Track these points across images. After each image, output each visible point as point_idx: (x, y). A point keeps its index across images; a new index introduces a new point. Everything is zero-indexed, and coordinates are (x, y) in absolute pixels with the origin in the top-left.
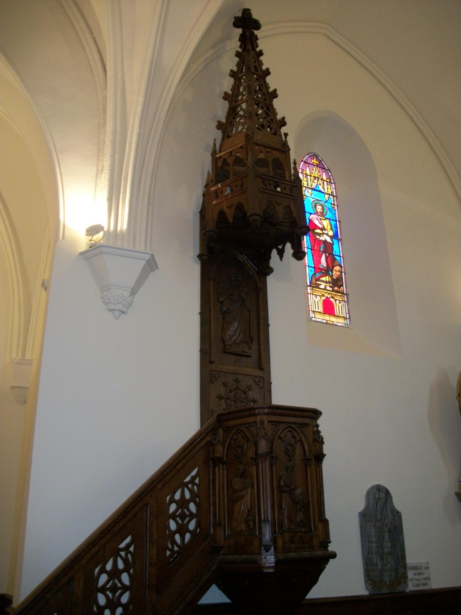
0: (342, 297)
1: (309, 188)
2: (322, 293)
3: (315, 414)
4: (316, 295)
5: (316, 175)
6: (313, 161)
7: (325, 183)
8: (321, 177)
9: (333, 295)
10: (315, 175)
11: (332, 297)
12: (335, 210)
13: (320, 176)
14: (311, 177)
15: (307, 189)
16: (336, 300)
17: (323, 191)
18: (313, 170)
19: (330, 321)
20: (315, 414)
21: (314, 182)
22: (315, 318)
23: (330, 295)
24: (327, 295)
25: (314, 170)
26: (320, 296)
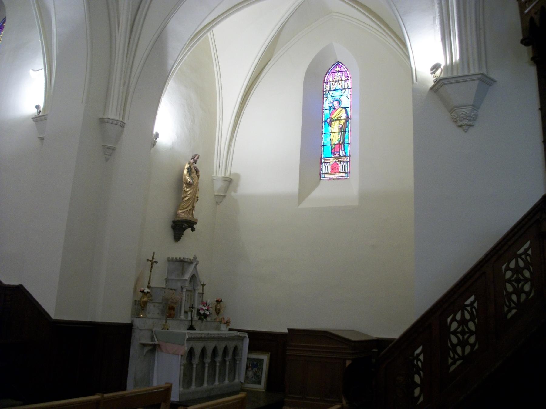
0: (345, 159)
1: (331, 91)
2: (331, 160)
3: (193, 231)
4: (327, 162)
5: (337, 79)
6: (336, 69)
7: (343, 81)
8: (341, 79)
9: (339, 160)
10: (336, 79)
11: (339, 161)
12: (349, 99)
13: (340, 78)
14: (333, 82)
15: (329, 92)
16: (341, 162)
17: (341, 88)
18: (335, 76)
19: (335, 177)
20: (193, 231)
21: (335, 85)
22: (324, 177)
23: (337, 160)
24: (334, 161)
25: (336, 76)
26: (330, 162)
